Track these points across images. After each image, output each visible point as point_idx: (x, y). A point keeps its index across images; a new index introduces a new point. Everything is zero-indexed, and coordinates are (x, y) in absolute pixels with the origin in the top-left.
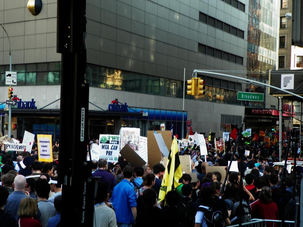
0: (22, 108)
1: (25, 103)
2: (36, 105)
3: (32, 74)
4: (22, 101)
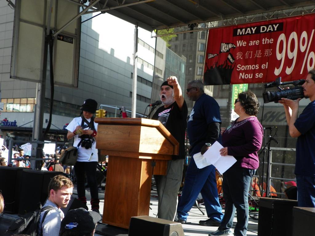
0: (8, 126)
1: (10, 123)
2: (17, 124)
3: (16, 105)
4: (9, 121)
